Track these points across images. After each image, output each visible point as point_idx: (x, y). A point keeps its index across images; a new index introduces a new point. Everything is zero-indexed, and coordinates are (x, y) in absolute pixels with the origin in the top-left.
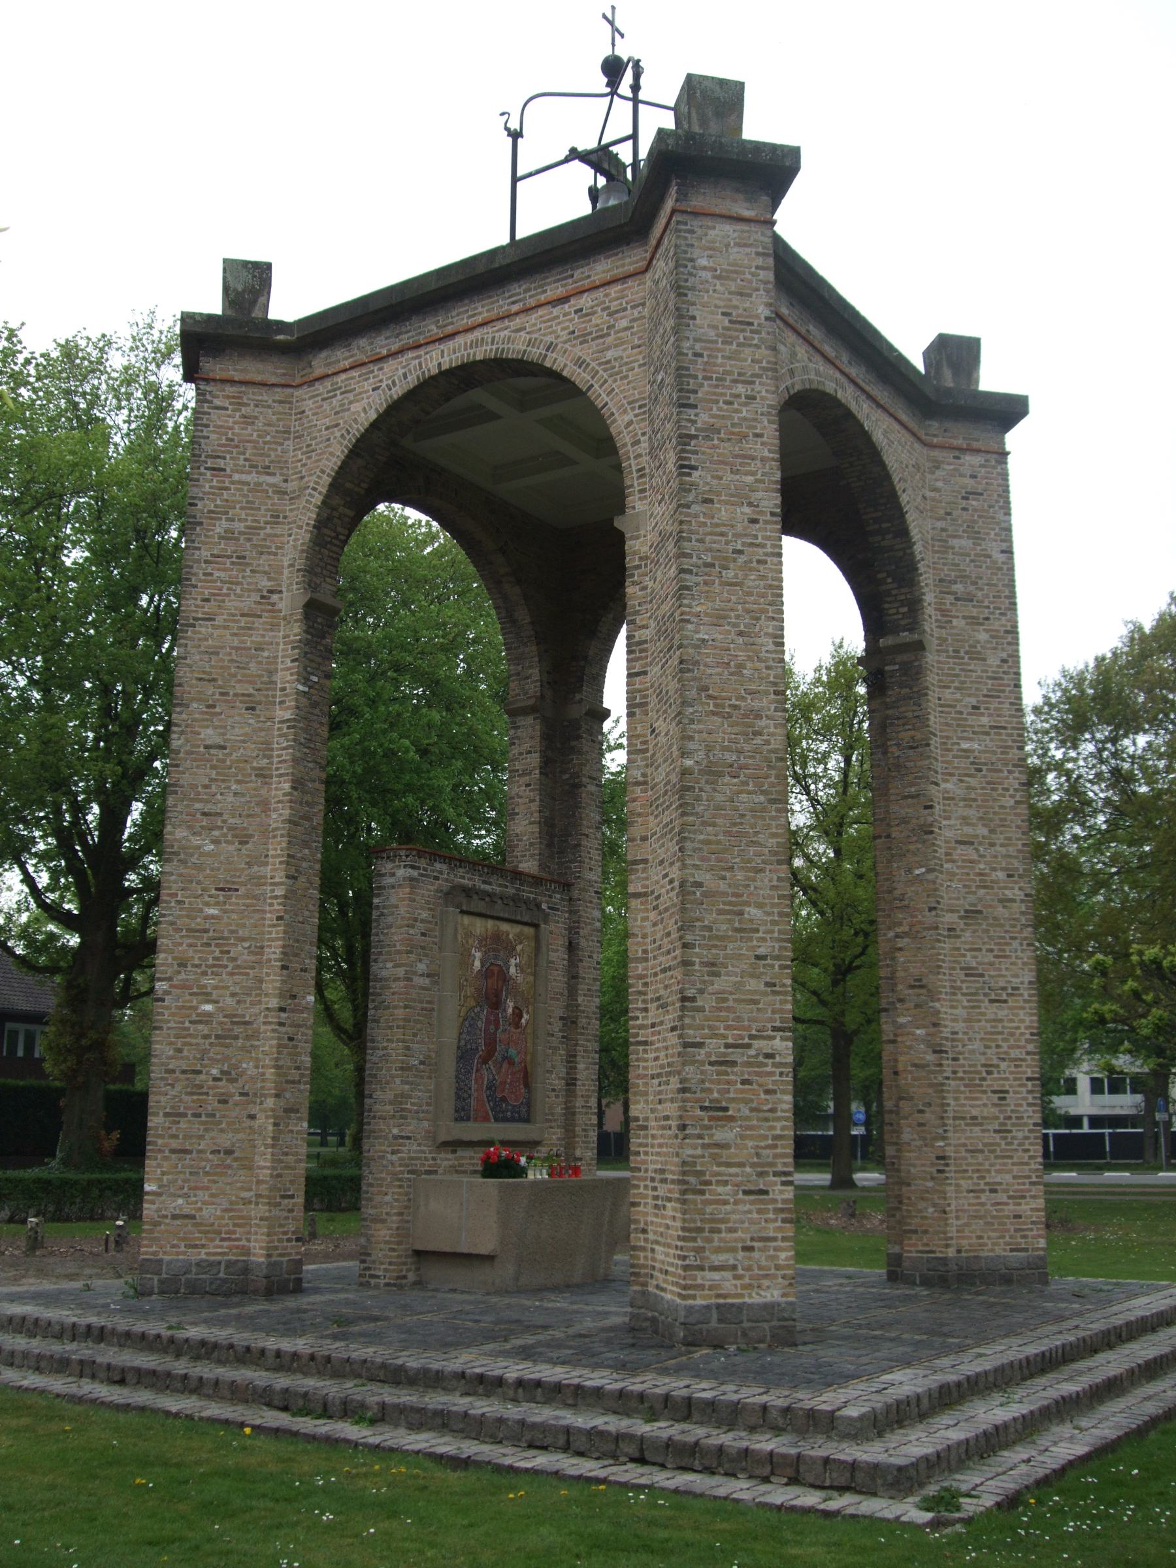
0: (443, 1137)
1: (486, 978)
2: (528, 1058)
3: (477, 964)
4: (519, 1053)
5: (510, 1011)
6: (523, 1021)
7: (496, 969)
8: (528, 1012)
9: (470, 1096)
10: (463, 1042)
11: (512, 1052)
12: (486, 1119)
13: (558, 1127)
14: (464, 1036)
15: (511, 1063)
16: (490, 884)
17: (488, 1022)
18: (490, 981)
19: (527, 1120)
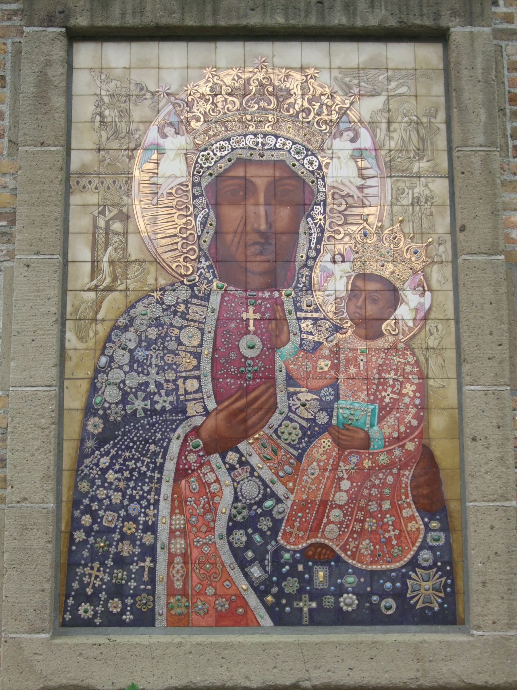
1: (216, 205)
14: (116, 375)
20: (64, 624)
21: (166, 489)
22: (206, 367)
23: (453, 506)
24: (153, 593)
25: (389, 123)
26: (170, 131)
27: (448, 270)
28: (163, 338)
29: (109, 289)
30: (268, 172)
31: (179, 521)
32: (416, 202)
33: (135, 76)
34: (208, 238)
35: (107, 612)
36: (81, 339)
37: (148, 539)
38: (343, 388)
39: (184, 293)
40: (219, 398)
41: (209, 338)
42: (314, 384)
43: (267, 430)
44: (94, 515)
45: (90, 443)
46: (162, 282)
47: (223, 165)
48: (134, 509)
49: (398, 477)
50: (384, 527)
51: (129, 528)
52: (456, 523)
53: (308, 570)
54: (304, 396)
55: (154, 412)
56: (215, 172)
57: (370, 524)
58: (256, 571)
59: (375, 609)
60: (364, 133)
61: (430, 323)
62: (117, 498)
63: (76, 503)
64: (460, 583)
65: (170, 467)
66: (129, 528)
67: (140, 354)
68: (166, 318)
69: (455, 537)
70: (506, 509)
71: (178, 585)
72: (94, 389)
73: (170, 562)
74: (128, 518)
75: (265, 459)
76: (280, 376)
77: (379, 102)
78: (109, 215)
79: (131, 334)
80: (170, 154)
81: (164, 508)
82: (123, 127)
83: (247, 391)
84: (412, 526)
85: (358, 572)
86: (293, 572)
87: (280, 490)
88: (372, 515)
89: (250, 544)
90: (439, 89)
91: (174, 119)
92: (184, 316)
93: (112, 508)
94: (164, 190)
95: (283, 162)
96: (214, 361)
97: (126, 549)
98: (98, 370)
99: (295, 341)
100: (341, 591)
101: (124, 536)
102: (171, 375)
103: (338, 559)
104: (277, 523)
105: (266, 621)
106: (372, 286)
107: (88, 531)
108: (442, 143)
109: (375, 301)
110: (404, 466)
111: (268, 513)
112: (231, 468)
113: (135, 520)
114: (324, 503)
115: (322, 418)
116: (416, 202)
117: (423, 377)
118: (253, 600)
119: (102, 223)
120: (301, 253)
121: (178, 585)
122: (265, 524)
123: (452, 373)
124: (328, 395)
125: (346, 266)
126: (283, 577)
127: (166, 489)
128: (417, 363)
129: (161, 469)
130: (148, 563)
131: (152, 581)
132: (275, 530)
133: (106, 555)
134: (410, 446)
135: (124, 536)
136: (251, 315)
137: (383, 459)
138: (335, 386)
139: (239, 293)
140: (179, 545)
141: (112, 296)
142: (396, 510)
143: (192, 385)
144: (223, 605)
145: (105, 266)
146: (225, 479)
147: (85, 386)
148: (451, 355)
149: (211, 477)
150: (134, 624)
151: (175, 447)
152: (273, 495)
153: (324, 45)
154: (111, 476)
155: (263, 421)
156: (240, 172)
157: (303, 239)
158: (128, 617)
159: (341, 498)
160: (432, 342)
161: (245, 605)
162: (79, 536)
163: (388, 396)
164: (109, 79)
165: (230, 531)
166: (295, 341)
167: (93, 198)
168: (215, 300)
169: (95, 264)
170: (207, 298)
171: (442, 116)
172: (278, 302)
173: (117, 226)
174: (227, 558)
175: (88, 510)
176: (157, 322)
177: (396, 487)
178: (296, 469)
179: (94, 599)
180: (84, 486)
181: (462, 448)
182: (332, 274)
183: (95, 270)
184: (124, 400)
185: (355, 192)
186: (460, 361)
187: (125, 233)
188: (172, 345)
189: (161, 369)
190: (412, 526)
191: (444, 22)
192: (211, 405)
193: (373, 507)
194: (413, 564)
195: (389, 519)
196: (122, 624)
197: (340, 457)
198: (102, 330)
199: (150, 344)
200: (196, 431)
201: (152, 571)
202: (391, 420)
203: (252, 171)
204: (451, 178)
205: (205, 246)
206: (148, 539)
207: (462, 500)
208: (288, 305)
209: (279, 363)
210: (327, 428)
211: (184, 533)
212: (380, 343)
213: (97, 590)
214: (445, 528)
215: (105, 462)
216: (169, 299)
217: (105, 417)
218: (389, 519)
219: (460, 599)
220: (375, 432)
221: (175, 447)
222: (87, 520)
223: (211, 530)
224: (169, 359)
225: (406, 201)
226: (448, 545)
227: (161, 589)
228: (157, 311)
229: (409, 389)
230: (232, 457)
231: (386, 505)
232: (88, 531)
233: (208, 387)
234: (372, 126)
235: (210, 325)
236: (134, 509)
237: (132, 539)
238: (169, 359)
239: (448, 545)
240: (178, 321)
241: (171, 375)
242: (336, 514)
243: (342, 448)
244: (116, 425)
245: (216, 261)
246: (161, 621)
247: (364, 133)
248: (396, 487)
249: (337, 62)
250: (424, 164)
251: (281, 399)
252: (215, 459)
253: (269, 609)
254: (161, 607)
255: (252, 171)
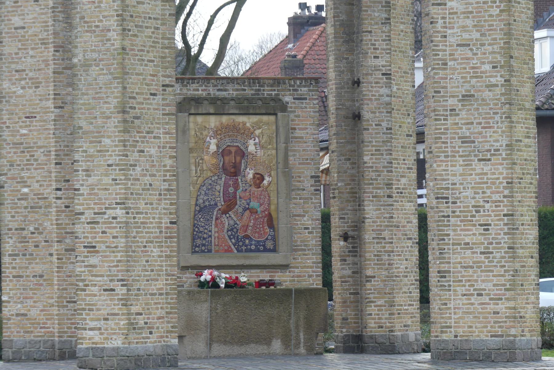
0: (183, 264)
1: (223, 156)
2: (273, 207)
3: (213, 148)
4: (261, 205)
5: (251, 176)
6: (265, 182)
7: (233, 150)
8: (270, 176)
9: (210, 236)
10: (201, 201)
11: (254, 204)
12: (229, 250)
13: (313, 254)
14: (202, 197)
15: (253, 211)
16: (226, 90)
17: (226, 186)
18: (227, 158)
19: (274, 250)
20: (193, 252)
21: (214, 222)
22: (222, 195)
23: (276, 226)
24: (211, 245)
25: (263, 136)
26: (212, 138)
27: (275, 172)
28: (212, 188)
29: (200, 177)
30: (235, 148)
31: (216, 230)
32: (268, 155)
33: (204, 124)
34: (221, 164)
35: (202, 249)
36: (194, 188)
37: (210, 233)
38: (252, 200)
39: (216, 178)
40: (225, 202)
41: (222, 188)
42: (245, 198)
43: (235, 209)
44: (198, 228)
45: (197, 212)
46: (211, 175)
47: (225, 146)
48: (207, 227)
49: (264, 220)
50: (261, 231)
51: (206, 231)
52: (276, 230)
53: (244, 240)
54: (243, 201)
55: (210, 205)
56: (223, 148)
57: (258, 230)
58: (233, 241)
59: (259, 249)
60: (257, 138)
61: (271, 185)
62: (203, 224)
63: (194, 226)
64: (277, 243)
65: (214, 217)
66: (206, 231)
67: (207, 192)
68: (212, 183)
69: (276, 233)
70: (287, 227)
71: (217, 244)
72: (197, 200)
73: (215, 239)
74: (206, 229)
75: (235, 216)
76: (238, 197)
77: (260, 131)
78: (199, 159)
79: (205, 187)
80: (212, 144)
81: (213, 226)
82: (201, 137)
83: (230, 200)
84: (267, 231)
85: (255, 241)
86: (241, 241)
87: (238, 222)
88: (257, 228)
89: (232, 235)
90: (274, 127)
91: (213, 135)
92: (216, 183)
93: (202, 227)
94: (211, 153)
95: (238, 146)
96: (223, 194)
97: (205, 236)
98: (198, 196)
99: (241, 188)
100: (251, 245)
101: (205, 233)
102: (214, 197)
103: (251, 238)
104: (238, 230)
105: (236, 251)
106: (258, 176)
107: (197, 232)
108: (275, 141)
109: (259, 179)
110: (265, 217)
111: (235, 228)
112: (228, 218)
113: (207, 229)
114: (248, 225)
115: (247, 206)
116: (268, 155)
117: (269, 197)
118: (233, 247)
119: (197, 161)
120: (243, 167)
121: (217, 244)
122: (235, 230)
123: (276, 196)
124: (248, 201)
125: (253, 171)
126: (239, 242)
127: (214, 222)
128: (268, 194)
129: (212, 218)
130: (210, 239)
131: (211, 243)
132: (237, 231)
133: (201, 237)
134: (266, 213)
135: (205, 233)
136: (231, 183)
137: (260, 216)
138: (250, 199)
139: (229, 177)
140: (216, 235)
141: (200, 178)
142: (263, 227)
143: (218, 199)
144: (226, 248)
145: (198, 171)
146: (226, 220)
147: (195, 199)
148: (276, 192)
149: (223, 220)
150: (207, 252)
151: (215, 213)
152: (237, 224)
153: (248, 116)
154: (201, 219)
155: (234, 207)
156: (228, 148)
157: (243, 165)
158: (206, 251)
159: (251, 224)
160: (272, 189)
161: (231, 248)
162: (195, 233)
163: (262, 201)
164: (197, 125)
165: (227, 231)
166: (241, 188)
167: (195, 155)
168: (223, 179)
169: (196, 170)
170: (221, 179)
171: (275, 134)
172: (237, 180)
173: (201, 161)
174: (227, 238)
175: (197, 227)
176: (210, 184)
177: (263, 222)
178: (241, 218)
179: (199, 247)
180: (196, 222)
181: (278, 214)
182: (249, 173)
183: (196, 173)
184: (204, 203)
185: (255, 153)
186: (278, 193)
187: (203, 163)
188: (214, 190)
189: (212, 195)
190: (267, 231)
191: (276, 112)
192: (223, 203)
193: (258, 226)
194: (267, 239)
195: (262, 229)
196: (205, 252)
197: (251, 215)
198: (198, 186)
199: (209, 189)
200: (220, 209)
201: (211, 241)
202: (262, 207)
203: (231, 149)
204: (277, 149)
205: (221, 166)
206: (210, 233)
207: (278, 225)
208: (240, 180)
209: (238, 194)
210: (248, 209)
211: (218, 232)
212: (260, 189)
213: (199, 245)
214: (274, 231)
215: (200, 216)
216: (213, 179)
217: (200, 206)
218: (262, 229)
219: (277, 247)
220: (259, 210)
221: (215, 213)
222: (197, 229)
223: (223, 231)
224: (213, 193)
225: (266, 155)
226: (274, 235)
227: (213, 244)
228: (210, 182)
229: (266, 200)
230: (228, 215)
231: (261, 226)
232: (197, 232)
233: (222, 199)
234: (259, 137)
235: (222, 185)
236: (207, 227)
237: (207, 233)
238: (213, 193)
239: (274, 235)
240: (215, 184)
241: (214, 197)
242: (250, 228)
243: (251, 213)
244: (202, 208)
245: (224, 170)
246: (213, 252)
247: (257, 138)
248: (263, 222)
249: (251, 120)
250: (270, 146)
251: (238, 202)
252: (224, 216)
253: (236, 249)
254: (213, 249)
255: (231, 149)
